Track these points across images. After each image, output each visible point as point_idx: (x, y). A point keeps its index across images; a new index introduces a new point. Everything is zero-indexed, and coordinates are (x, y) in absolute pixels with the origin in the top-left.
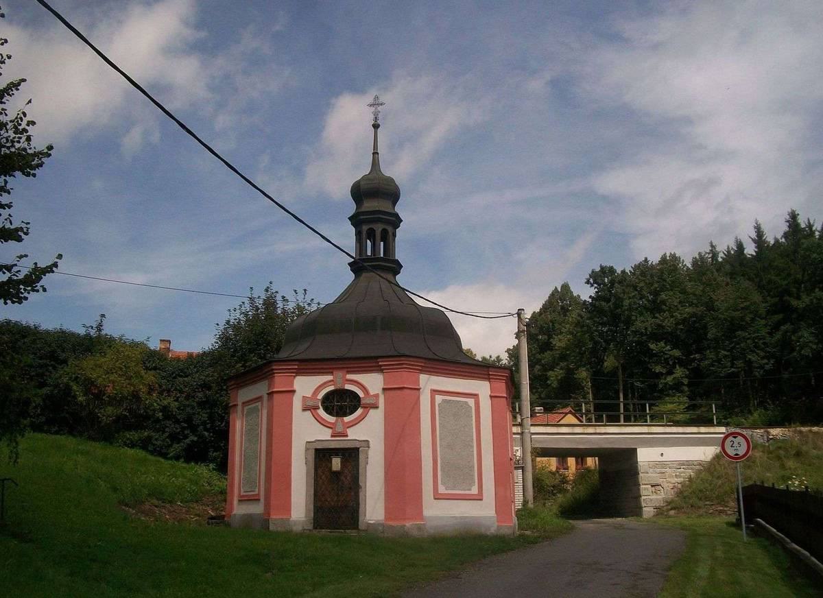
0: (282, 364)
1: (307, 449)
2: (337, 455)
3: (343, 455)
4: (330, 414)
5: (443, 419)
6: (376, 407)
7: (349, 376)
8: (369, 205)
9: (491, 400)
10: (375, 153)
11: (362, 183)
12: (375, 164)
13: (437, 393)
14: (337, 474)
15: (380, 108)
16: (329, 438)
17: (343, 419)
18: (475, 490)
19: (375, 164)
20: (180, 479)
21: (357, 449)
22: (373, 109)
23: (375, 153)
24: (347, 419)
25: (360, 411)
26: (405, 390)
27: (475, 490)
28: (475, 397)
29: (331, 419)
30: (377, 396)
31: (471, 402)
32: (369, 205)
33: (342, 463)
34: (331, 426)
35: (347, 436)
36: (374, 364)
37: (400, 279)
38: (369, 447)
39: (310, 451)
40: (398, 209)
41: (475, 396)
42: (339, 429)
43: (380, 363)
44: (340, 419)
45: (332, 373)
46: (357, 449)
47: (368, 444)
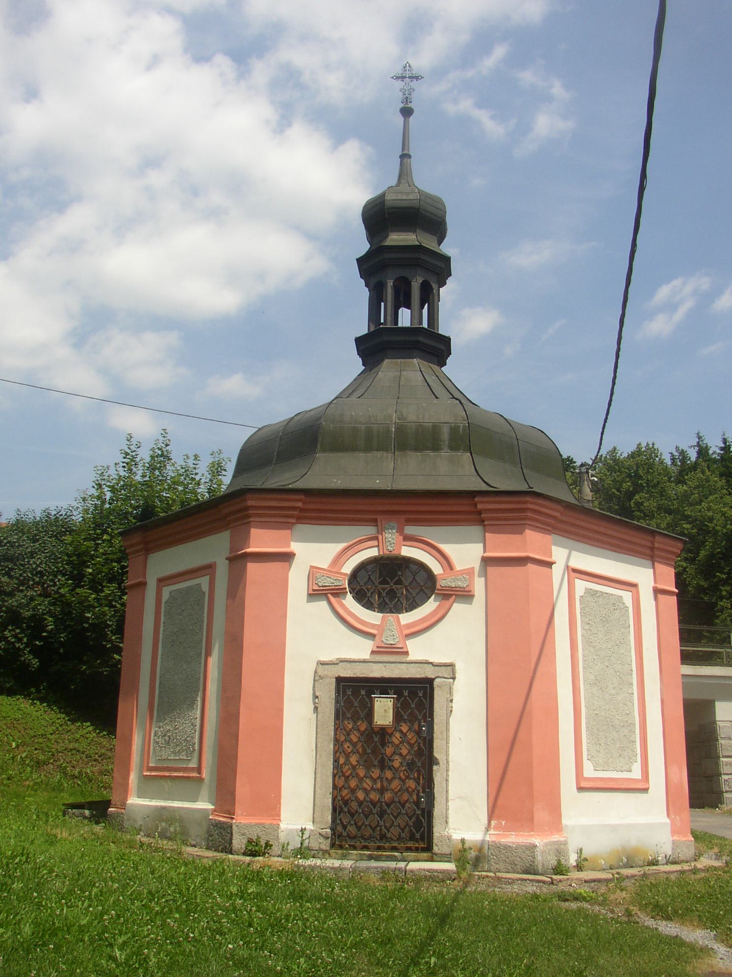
0: (271, 496)
1: (317, 678)
2: (384, 691)
3: (399, 692)
4: (369, 605)
5: (587, 627)
6: (466, 595)
7: (410, 530)
8: (396, 238)
9: (656, 599)
10: (405, 156)
11: (388, 197)
12: (404, 174)
13: (577, 575)
14: (383, 731)
15: (414, 84)
16: (367, 656)
17: (398, 619)
18: (636, 773)
19: (404, 174)
20: (291, 859)
21: (429, 682)
22: (399, 84)
23: (405, 156)
24: (406, 618)
25: (431, 605)
26: (531, 567)
27: (636, 773)
28: (633, 589)
29: (373, 617)
30: (470, 572)
31: (627, 596)
32: (396, 238)
33: (395, 707)
34: (374, 631)
35: (407, 653)
36: (466, 508)
37: (452, 368)
38: (454, 678)
39: (327, 680)
40: (447, 248)
41: (632, 586)
42: (391, 638)
43: (479, 506)
44: (391, 617)
45: (375, 521)
46: (429, 682)
47: (454, 672)
